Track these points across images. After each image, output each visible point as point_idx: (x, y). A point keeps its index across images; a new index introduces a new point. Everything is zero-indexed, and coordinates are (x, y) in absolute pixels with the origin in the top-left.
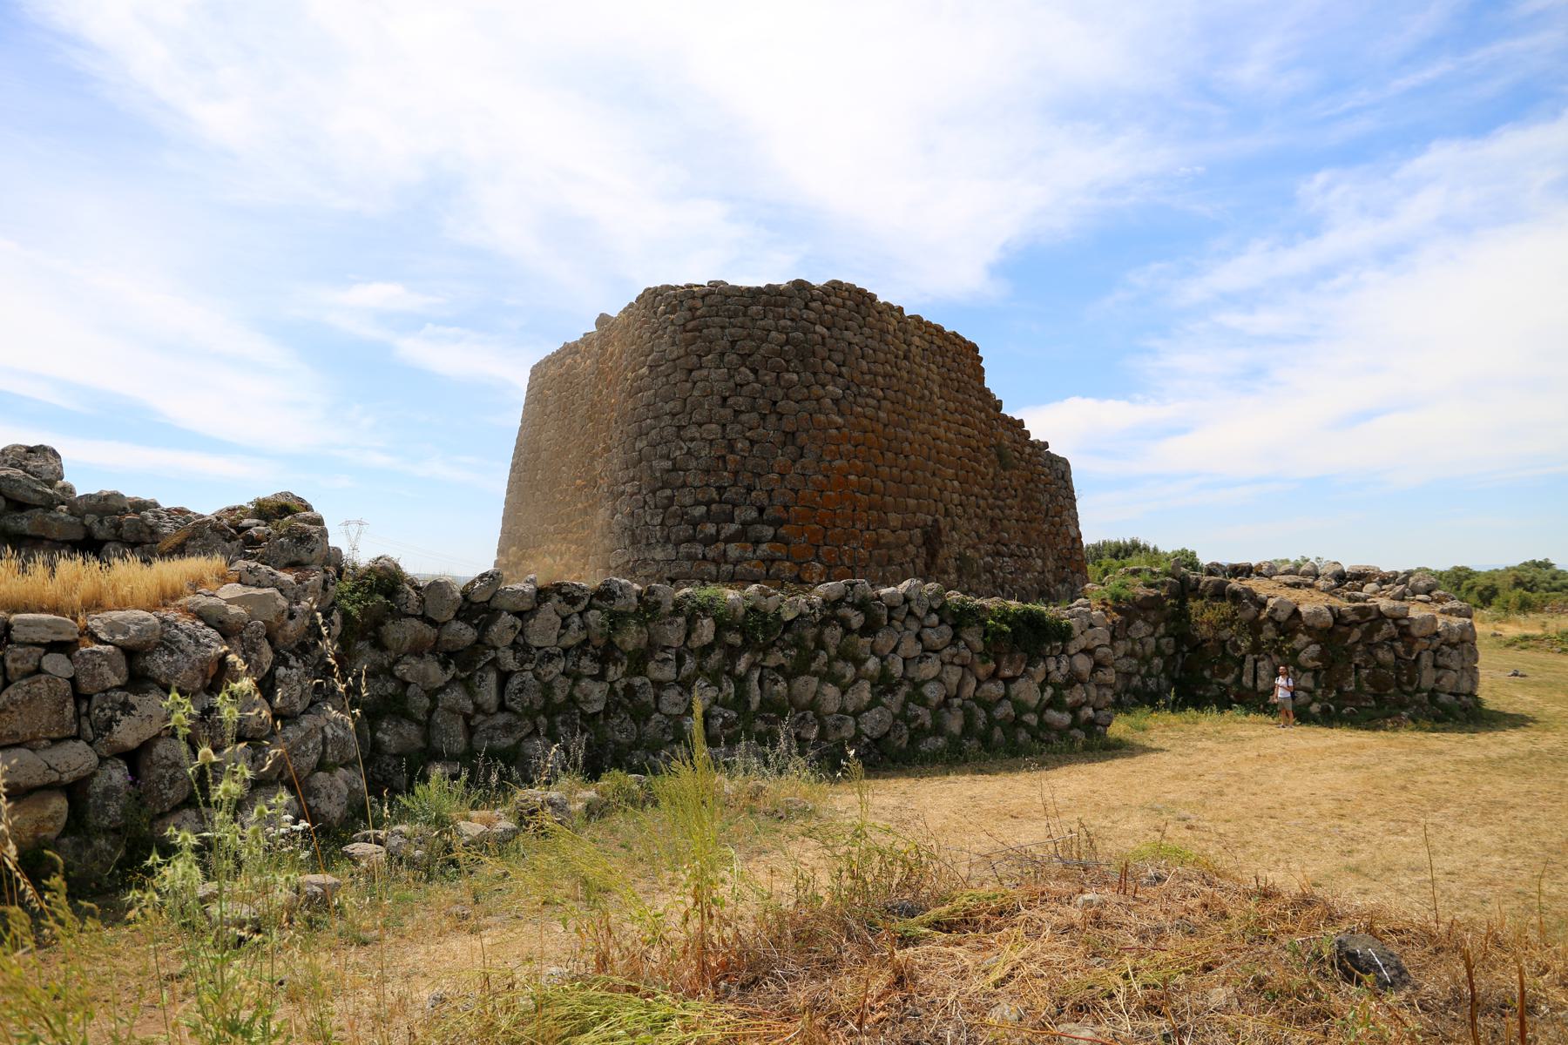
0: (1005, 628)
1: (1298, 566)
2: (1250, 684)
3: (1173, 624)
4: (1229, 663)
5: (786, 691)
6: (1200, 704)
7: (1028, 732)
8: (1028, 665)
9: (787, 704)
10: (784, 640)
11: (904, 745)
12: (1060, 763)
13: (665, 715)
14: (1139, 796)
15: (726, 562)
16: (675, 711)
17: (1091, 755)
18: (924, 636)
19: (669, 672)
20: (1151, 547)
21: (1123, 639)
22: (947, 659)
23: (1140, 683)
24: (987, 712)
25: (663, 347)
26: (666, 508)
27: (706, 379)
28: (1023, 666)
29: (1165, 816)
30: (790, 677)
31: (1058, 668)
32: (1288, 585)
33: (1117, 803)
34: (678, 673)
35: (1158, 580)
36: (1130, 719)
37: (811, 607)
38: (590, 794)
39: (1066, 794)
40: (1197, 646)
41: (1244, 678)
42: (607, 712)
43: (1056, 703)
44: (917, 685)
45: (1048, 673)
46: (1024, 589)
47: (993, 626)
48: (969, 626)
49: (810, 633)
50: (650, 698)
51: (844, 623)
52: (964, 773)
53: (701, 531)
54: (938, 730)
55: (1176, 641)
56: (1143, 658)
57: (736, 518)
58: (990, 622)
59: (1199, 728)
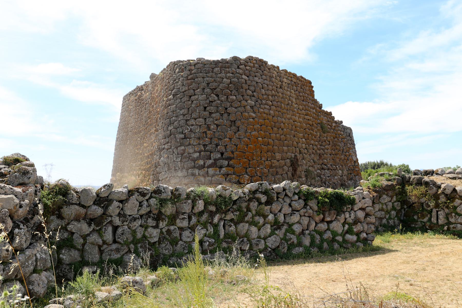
0: (327, 200)
1: (455, 170)
2: (435, 222)
3: (399, 197)
4: (425, 213)
5: (235, 230)
6: (413, 230)
7: (338, 244)
8: (337, 215)
9: (236, 235)
10: (233, 208)
11: (286, 251)
12: (353, 257)
13: (185, 242)
14: (388, 271)
15: (208, 176)
16: (188, 240)
17: (366, 253)
18: (292, 205)
19: (185, 224)
20: (389, 164)
21: (378, 203)
22: (302, 214)
23: (386, 222)
24: (320, 236)
25: (179, 87)
26: (182, 154)
27: (197, 100)
28: (335, 216)
29: (400, 280)
30: (236, 224)
31: (350, 217)
32: (451, 178)
33: (378, 274)
34: (189, 224)
35: (392, 178)
36: (382, 238)
37: (244, 194)
38: (153, 277)
39: (356, 271)
40: (411, 206)
41: (432, 219)
42: (159, 242)
43: (349, 231)
44: (290, 226)
45: (346, 219)
46: (334, 183)
47: (321, 199)
48: (311, 200)
49: (244, 205)
50: (178, 235)
51: (258, 200)
52: (311, 262)
53: (197, 164)
54: (300, 244)
55: (401, 204)
56: (387, 211)
57: (211, 157)
58: (320, 198)
59: (413, 241)
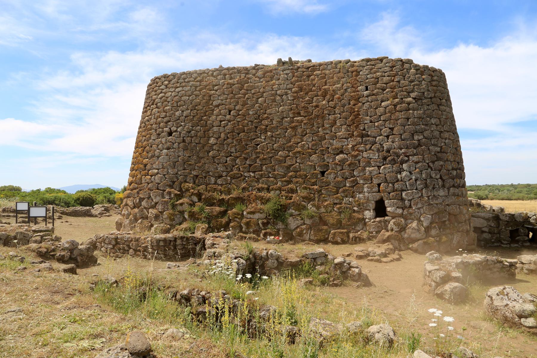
25: (422, 91)
26: (440, 170)
53: (456, 182)
